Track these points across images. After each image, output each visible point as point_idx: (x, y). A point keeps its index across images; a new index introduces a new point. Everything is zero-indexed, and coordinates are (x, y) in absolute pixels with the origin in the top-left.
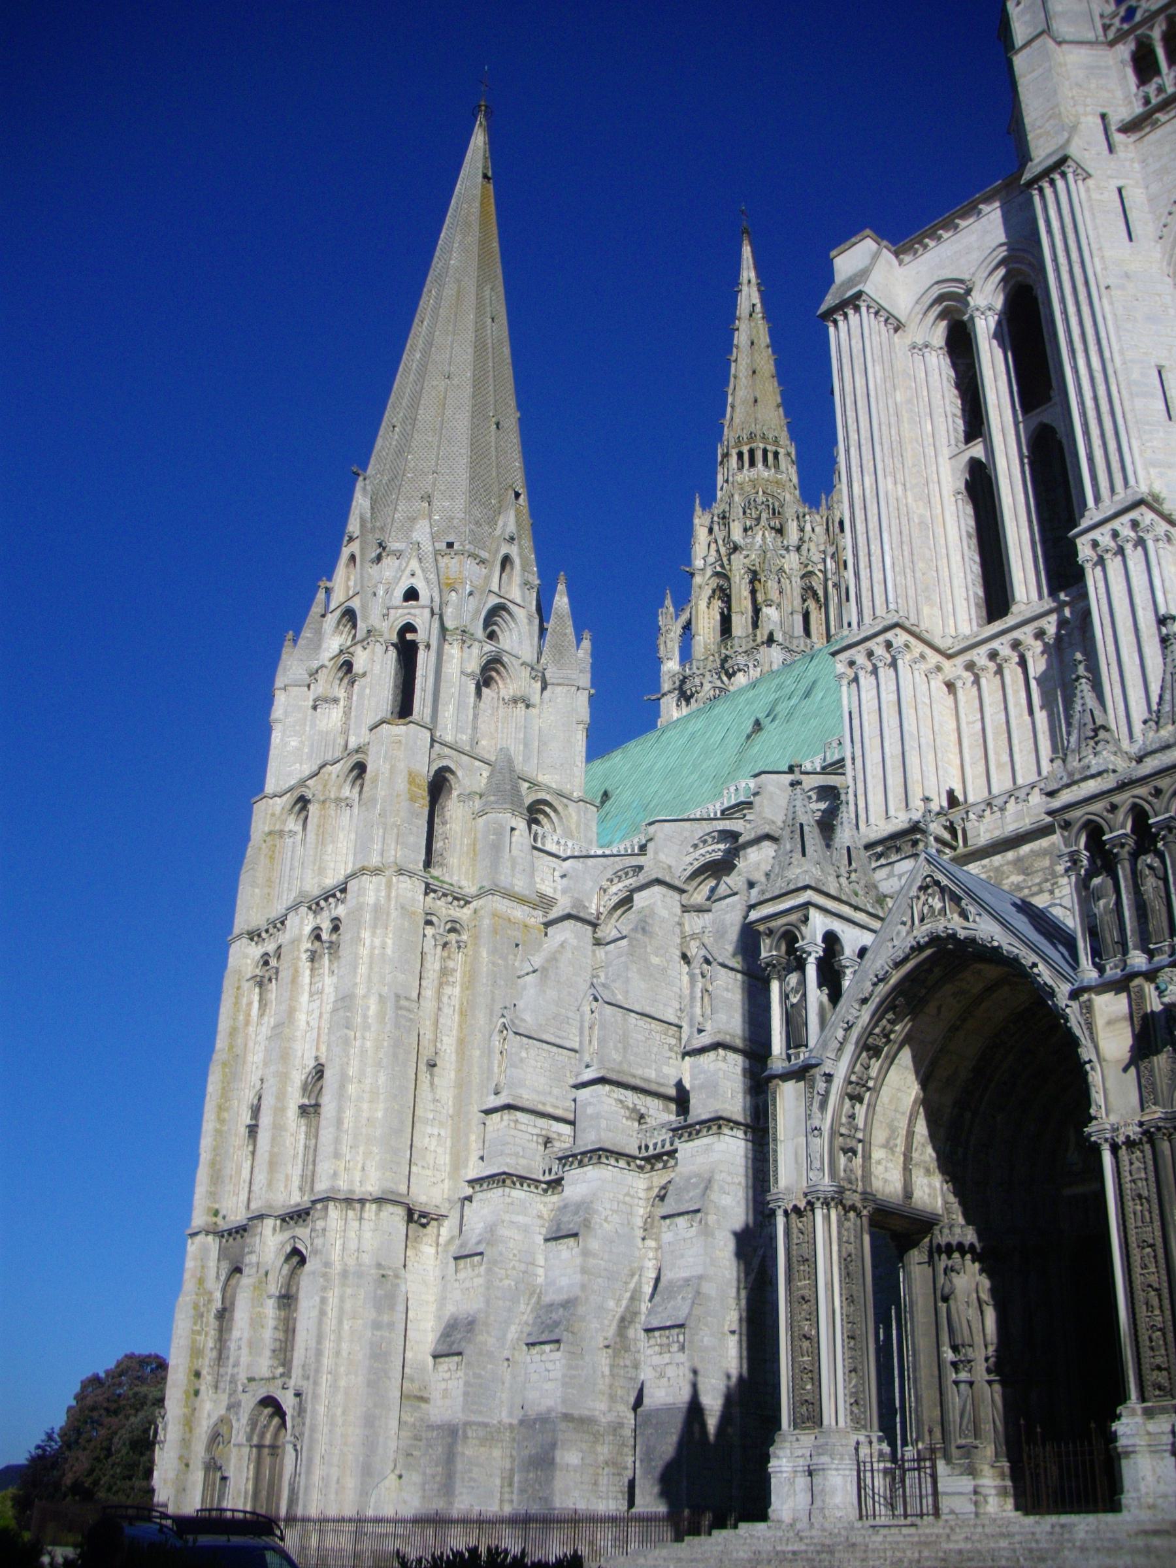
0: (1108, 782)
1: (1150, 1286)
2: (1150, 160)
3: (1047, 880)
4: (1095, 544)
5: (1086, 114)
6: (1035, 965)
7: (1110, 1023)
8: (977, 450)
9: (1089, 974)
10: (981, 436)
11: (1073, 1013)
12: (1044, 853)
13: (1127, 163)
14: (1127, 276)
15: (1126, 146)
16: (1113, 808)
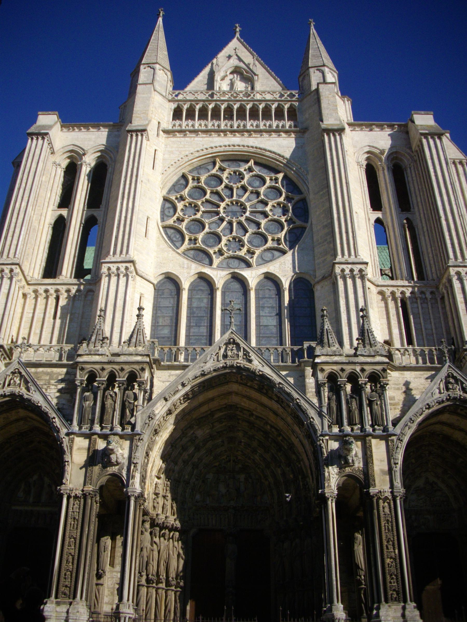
0: (105, 359)
1: (70, 554)
2: (168, 146)
3: (46, 385)
4: (109, 269)
5: (154, 119)
6: (54, 418)
7: (79, 449)
8: (64, 212)
9: (75, 428)
10: (67, 208)
11: (66, 441)
12: (48, 374)
13: (161, 143)
14: (148, 181)
15: (162, 137)
16: (103, 369)
